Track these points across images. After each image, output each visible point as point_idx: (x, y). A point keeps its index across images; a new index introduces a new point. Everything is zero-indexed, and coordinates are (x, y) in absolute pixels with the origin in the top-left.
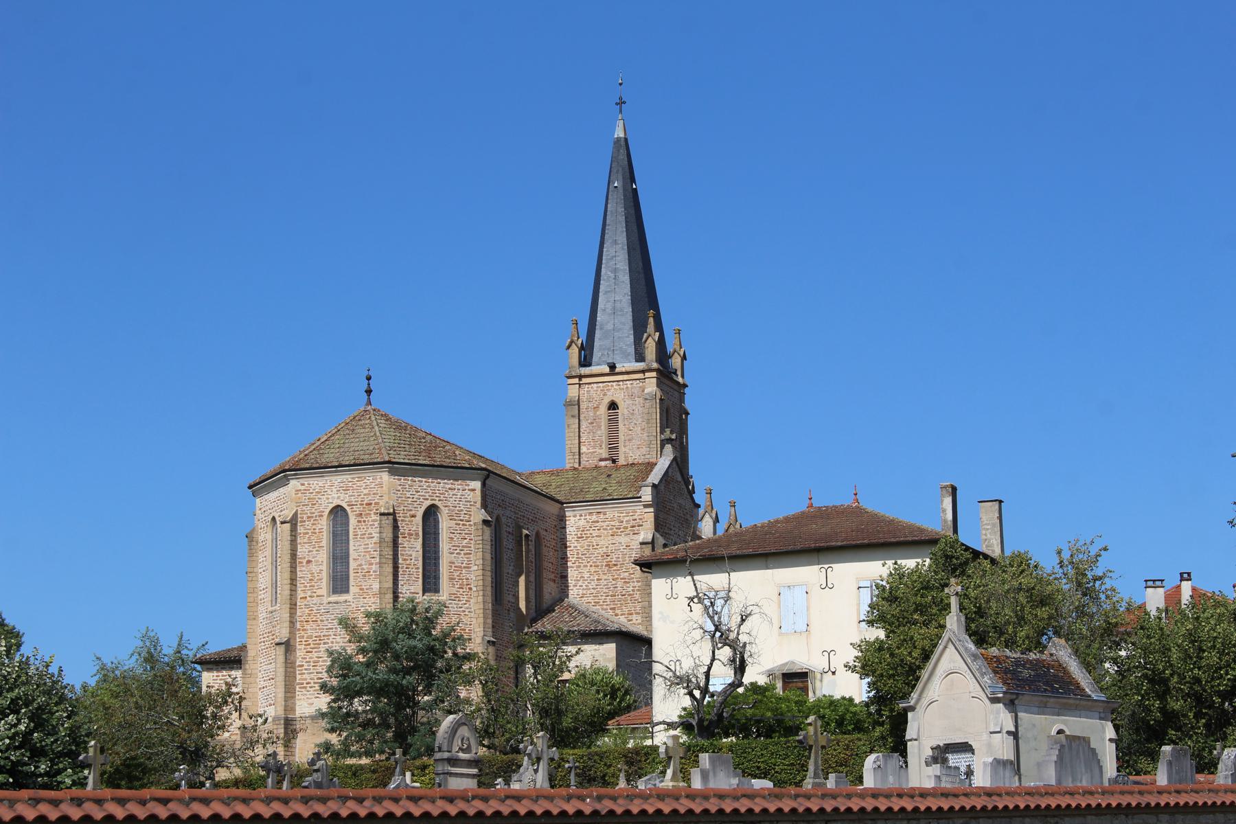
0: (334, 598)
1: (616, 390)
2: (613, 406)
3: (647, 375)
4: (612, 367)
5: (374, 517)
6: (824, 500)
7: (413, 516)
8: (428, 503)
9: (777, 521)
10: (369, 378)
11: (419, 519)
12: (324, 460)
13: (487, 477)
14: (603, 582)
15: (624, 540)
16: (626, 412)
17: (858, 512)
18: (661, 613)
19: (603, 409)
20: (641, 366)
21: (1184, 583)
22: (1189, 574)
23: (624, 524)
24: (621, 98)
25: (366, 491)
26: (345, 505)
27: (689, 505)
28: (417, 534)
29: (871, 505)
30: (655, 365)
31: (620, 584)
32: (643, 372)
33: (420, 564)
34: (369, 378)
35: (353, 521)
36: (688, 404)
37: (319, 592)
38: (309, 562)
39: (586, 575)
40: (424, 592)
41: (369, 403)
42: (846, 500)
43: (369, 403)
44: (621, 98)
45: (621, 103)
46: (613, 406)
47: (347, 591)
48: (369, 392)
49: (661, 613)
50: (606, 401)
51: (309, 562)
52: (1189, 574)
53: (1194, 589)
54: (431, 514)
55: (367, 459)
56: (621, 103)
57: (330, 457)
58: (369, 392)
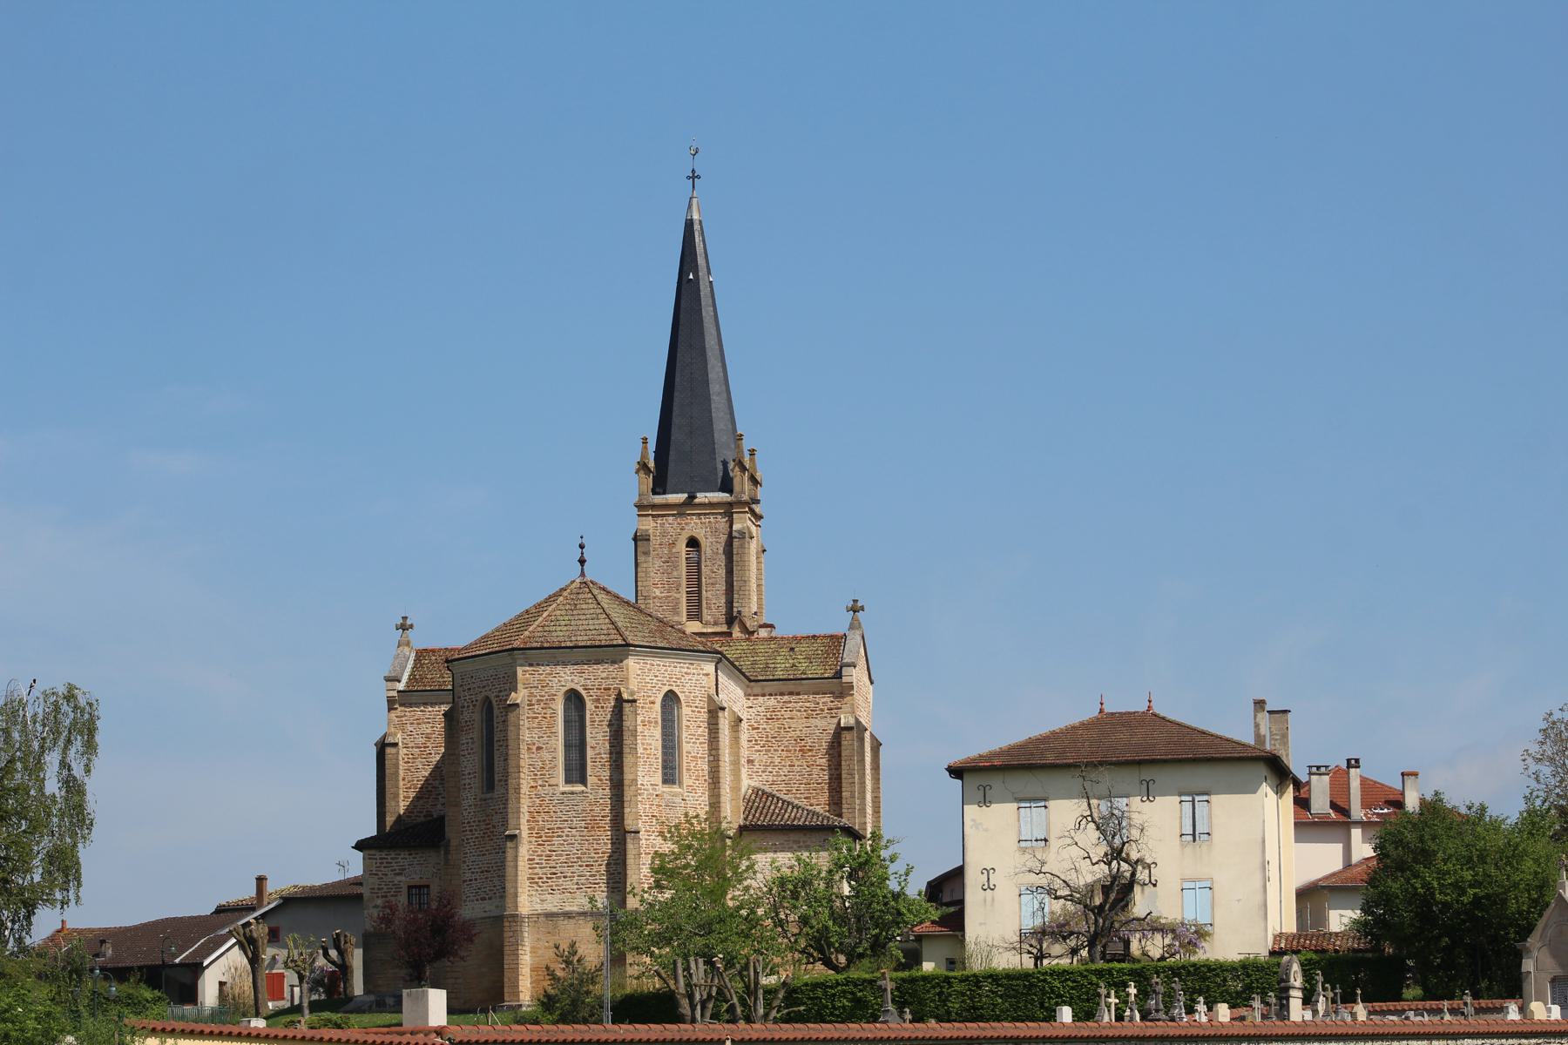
0: (568, 788)
2: (693, 543)
6: (1119, 704)
8: (666, 689)
9: (1074, 728)
10: (582, 547)
14: (797, 769)
16: (709, 551)
17: (1150, 719)
19: (682, 547)
21: (1352, 771)
22: (1357, 761)
26: (580, 690)
34: (582, 547)
35: (589, 705)
38: (539, 748)
39: (777, 760)
40: (665, 781)
41: (583, 574)
43: (583, 574)
45: (694, 177)
48: (582, 562)
51: (539, 748)
52: (1357, 761)
53: (1364, 782)
54: (671, 699)
56: (694, 177)
58: (582, 562)
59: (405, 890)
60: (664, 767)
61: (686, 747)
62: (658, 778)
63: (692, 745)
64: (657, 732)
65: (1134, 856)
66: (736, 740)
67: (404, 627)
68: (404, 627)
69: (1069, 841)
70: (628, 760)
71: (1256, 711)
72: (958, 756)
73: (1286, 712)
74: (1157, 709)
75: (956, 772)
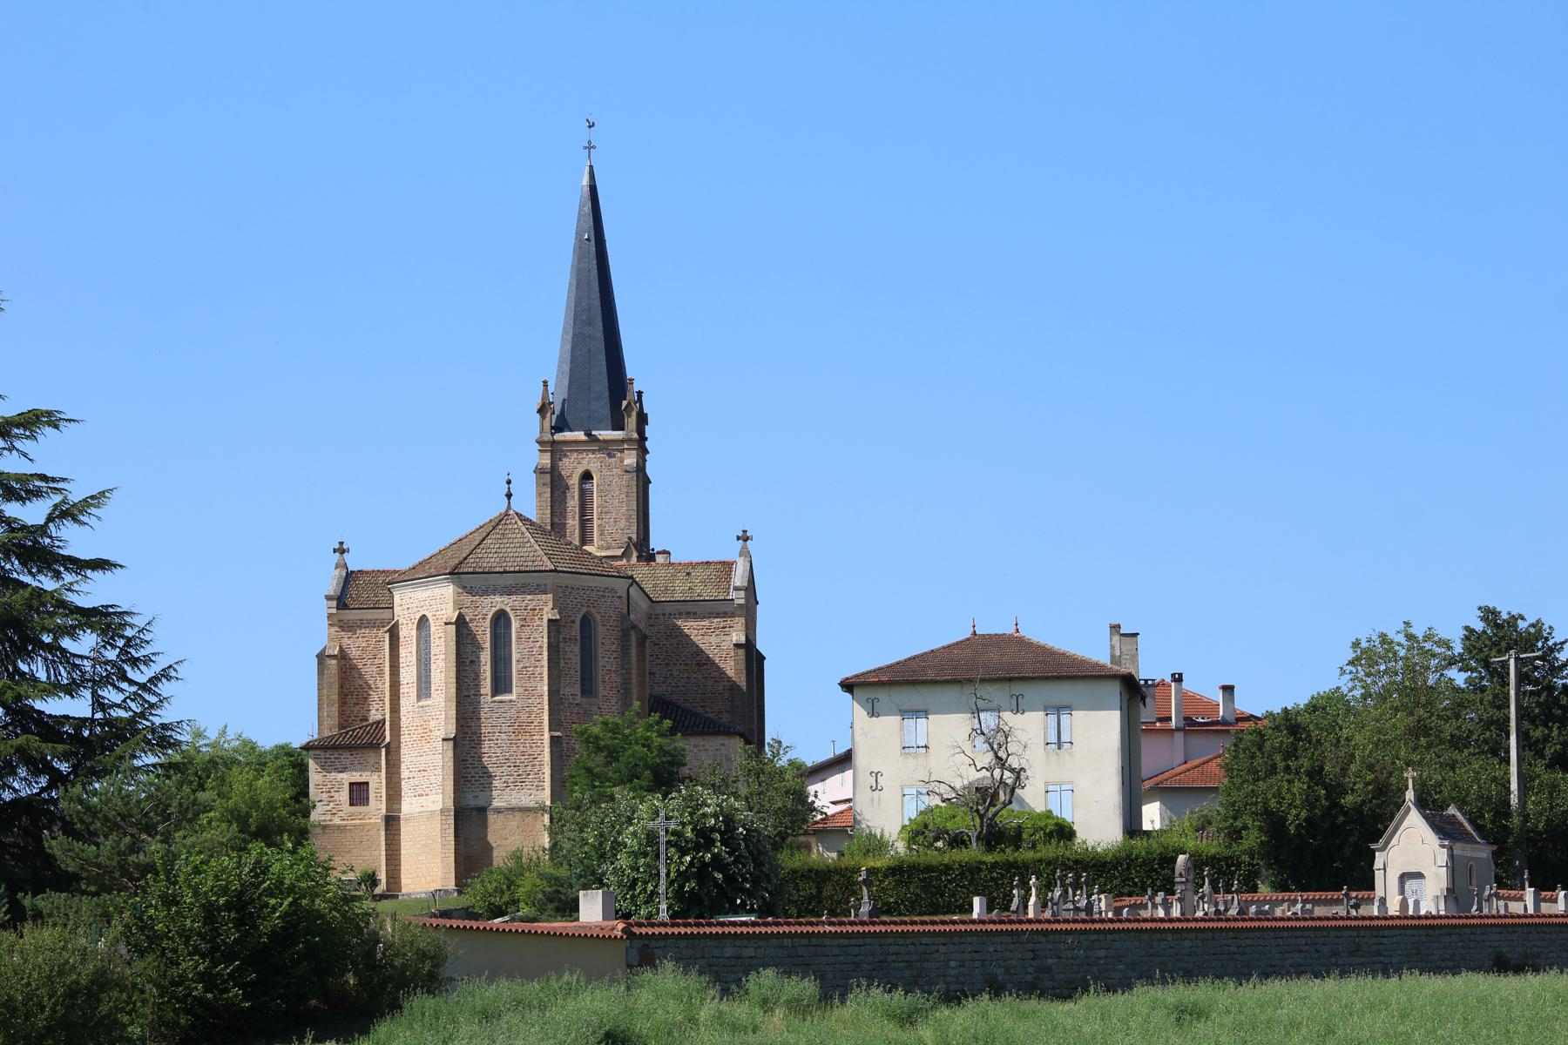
1: (591, 462)
4: (589, 434)
8: (584, 610)
10: (509, 482)
11: (577, 625)
17: (1015, 642)
20: (618, 434)
29: (1028, 633)
30: (635, 436)
31: (709, 683)
32: (623, 441)
34: (509, 482)
35: (515, 625)
36: (650, 470)
41: (509, 507)
42: (1009, 629)
43: (509, 507)
46: (587, 476)
48: (509, 496)
50: (580, 470)
58: (509, 496)
59: (346, 786)
60: (583, 679)
61: (601, 662)
62: (577, 689)
64: (577, 649)
67: (341, 550)
68: (341, 550)
70: (998, 686)
72: (849, 672)
74: (1022, 633)
75: (848, 686)
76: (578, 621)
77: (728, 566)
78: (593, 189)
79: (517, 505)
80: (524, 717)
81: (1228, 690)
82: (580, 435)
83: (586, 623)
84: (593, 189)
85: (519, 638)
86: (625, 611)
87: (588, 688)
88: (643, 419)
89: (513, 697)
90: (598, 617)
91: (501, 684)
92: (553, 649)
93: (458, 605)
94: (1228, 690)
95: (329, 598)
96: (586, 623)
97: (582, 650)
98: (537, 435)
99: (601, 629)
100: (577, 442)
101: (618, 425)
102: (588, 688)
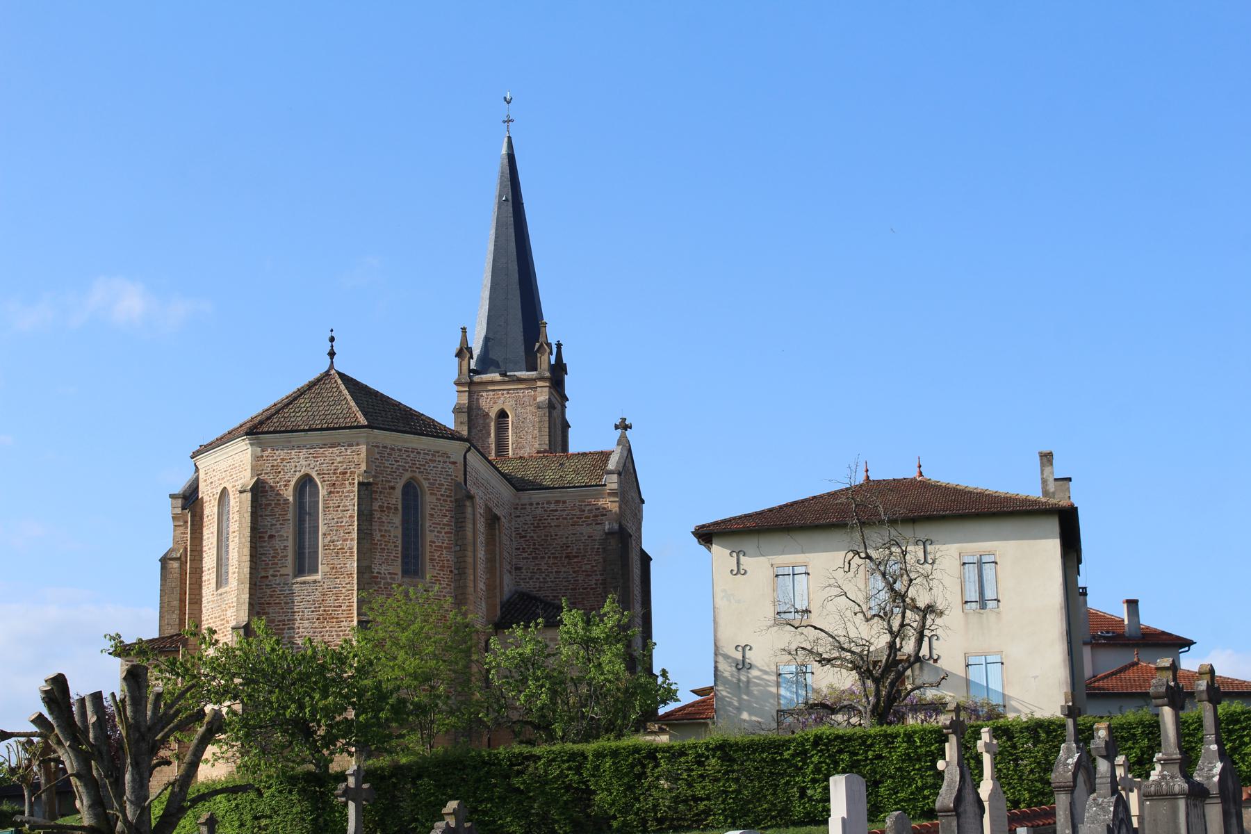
3: (539, 384)
5: (348, 488)
7: (393, 488)
8: (408, 475)
10: (332, 339)
11: (398, 492)
12: (290, 425)
13: (469, 450)
15: (586, 530)
18: (724, 591)
20: (533, 374)
23: (586, 514)
24: (508, 116)
25: (339, 459)
26: (314, 475)
27: (638, 500)
28: (396, 509)
31: (581, 578)
32: (535, 380)
33: (399, 542)
34: (332, 339)
35: (322, 492)
36: (569, 416)
37: (283, 571)
38: (271, 537)
39: (544, 568)
42: (911, 473)
44: (508, 116)
47: (316, 571)
48: (332, 354)
49: (724, 591)
51: (271, 537)
55: (342, 422)
57: (297, 417)
58: (332, 354)
61: (429, 537)
62: (397, 567)
63: (435, 535)
64: (397, 520)
65: (921, 604)
66: (491, 540)
69: (837, 591)
71: (1042, 465)
73: (1070, 479)
75: (706, 535)
76: (400, 486)
77: (606, 455)
78: (511, 157)
79: (340, 365)
80: (330, 600)
81: (1132, 604)
82: (497, 377)
83: (411, 492)
84: (511, 157)
85: (326, 507)
86: (461, 479)
87: (412, 565)
88: (559, 370)
89: (319, 577)
90: (425, 484)
91: (305, 562)
92: (365, 517)
93: (255, 470)
94: (1132, 604)
95: (173, 497)
96: (411, 492)
97: (405, 521)
98: (455, 377)
99: (429, 498)
100: (493, 383)
101: (532, 366)
102: (412, 565)
